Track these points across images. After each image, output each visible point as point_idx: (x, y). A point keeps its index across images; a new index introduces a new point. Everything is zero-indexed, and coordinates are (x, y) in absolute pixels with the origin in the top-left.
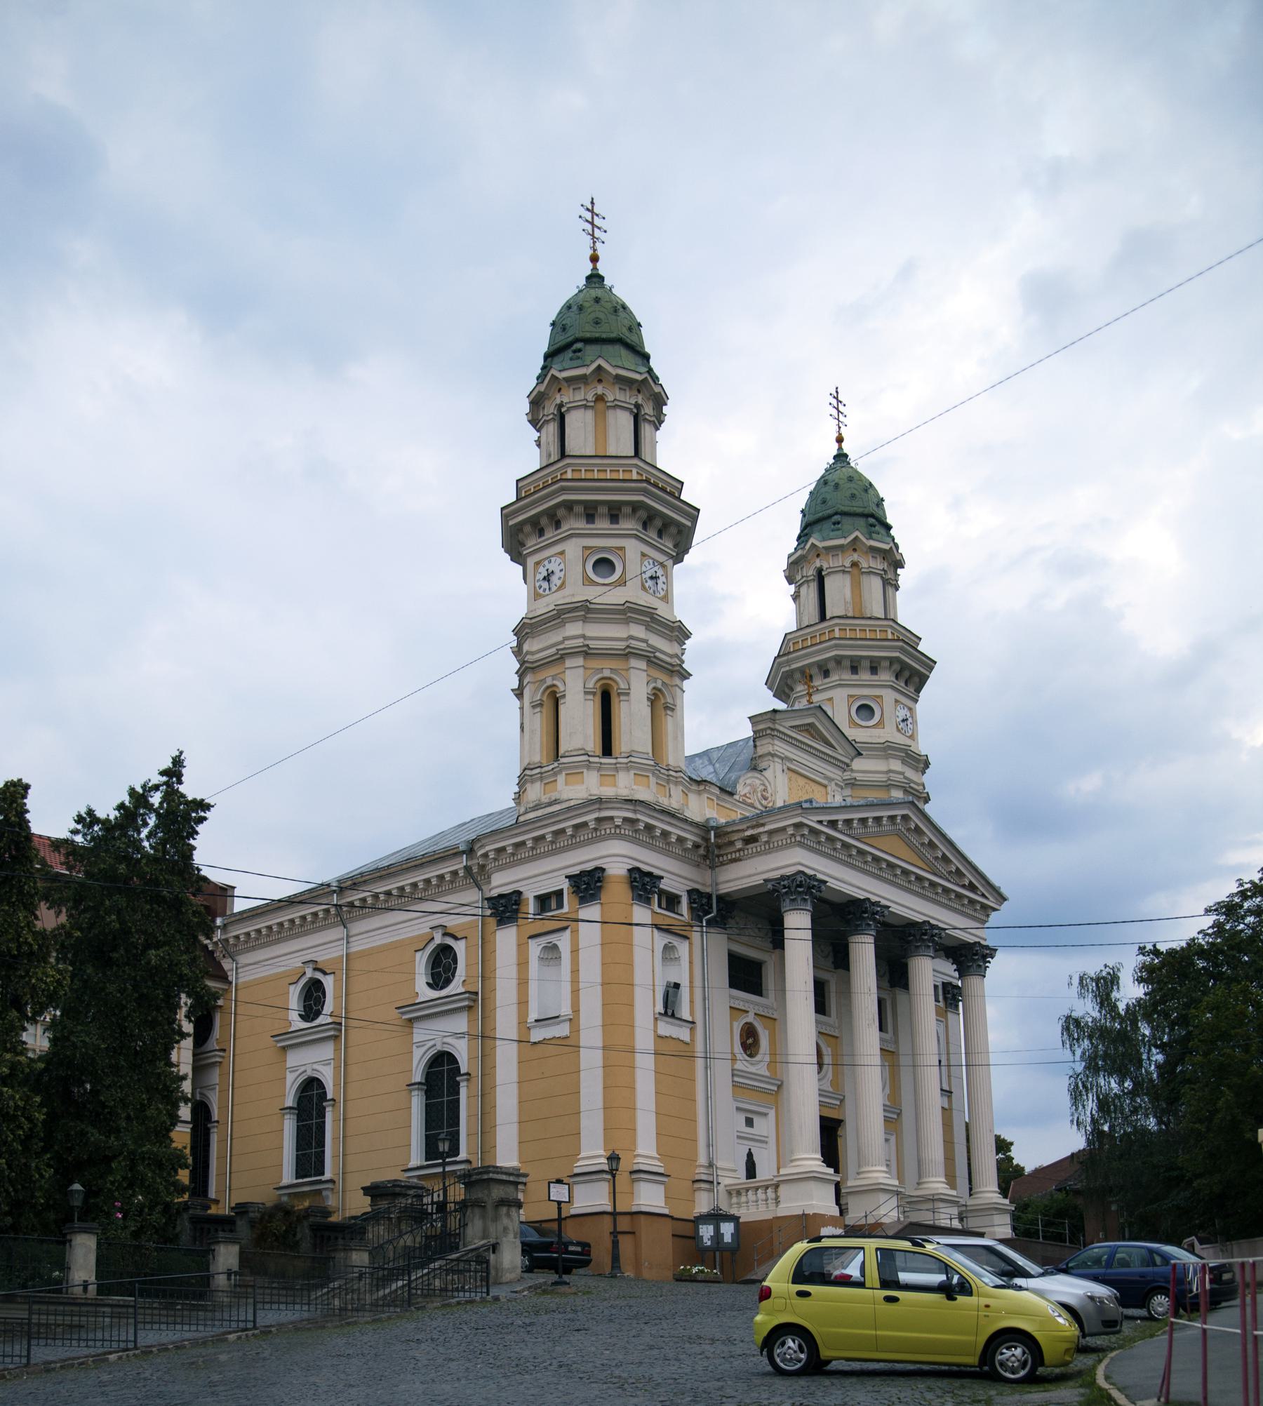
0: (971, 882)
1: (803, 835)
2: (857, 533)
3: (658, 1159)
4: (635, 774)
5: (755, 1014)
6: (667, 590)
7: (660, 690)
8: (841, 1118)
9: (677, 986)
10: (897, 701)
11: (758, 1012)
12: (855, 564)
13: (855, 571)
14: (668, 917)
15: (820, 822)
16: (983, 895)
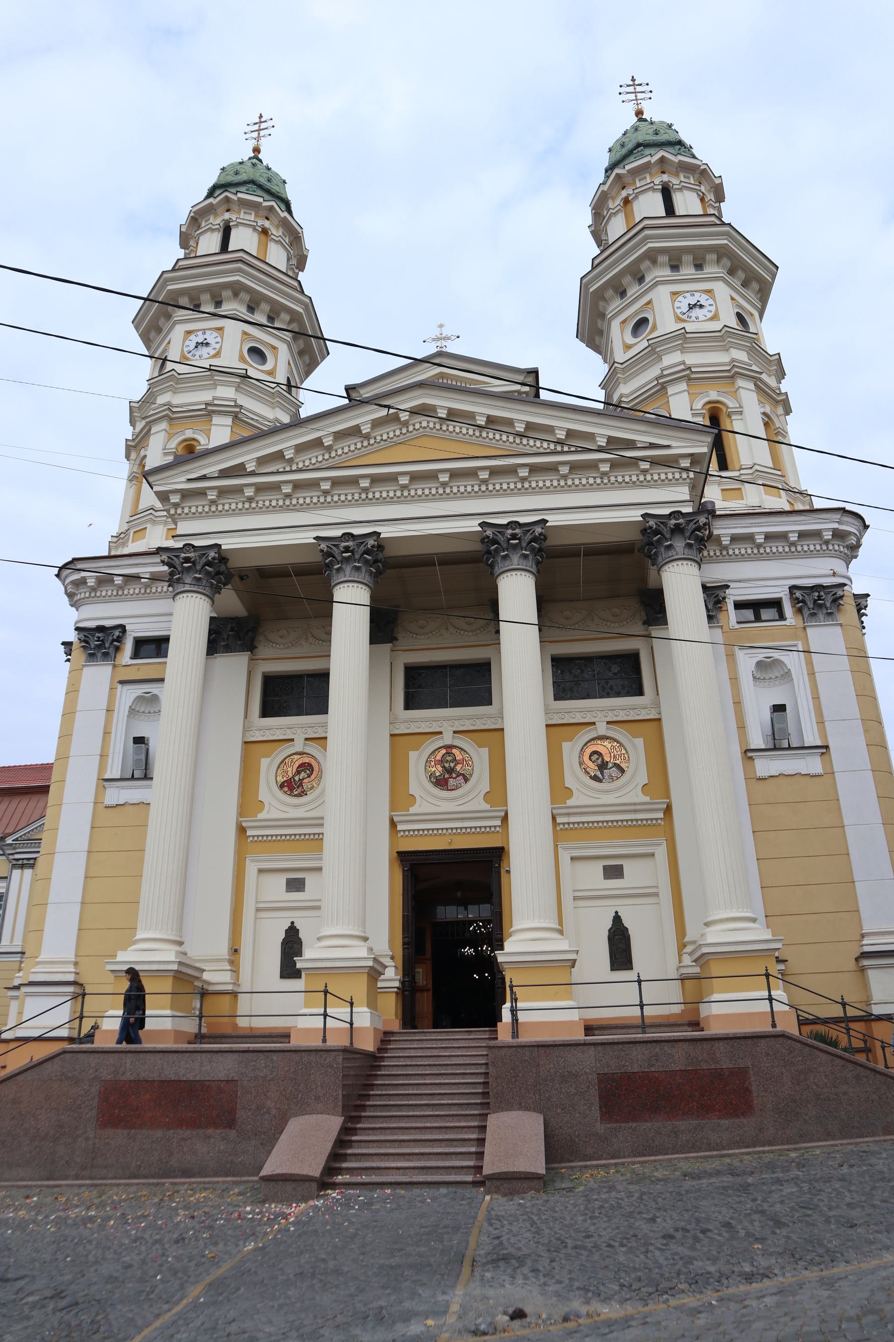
0: (611, 440)
1: (176, 505)
2: (617, 171)
3: (76, 964)
4: (134, 532)
5: (306, 739)
6: (221, 347)
7: (194, 439)
8: (499, 845)
9: (139, 741)
10: (674, 294)
11: (307, 736)
12: (627, 201)
13: (629, 206)
14: (147, 666)
15: (204, 478)
16: (652, 446)
